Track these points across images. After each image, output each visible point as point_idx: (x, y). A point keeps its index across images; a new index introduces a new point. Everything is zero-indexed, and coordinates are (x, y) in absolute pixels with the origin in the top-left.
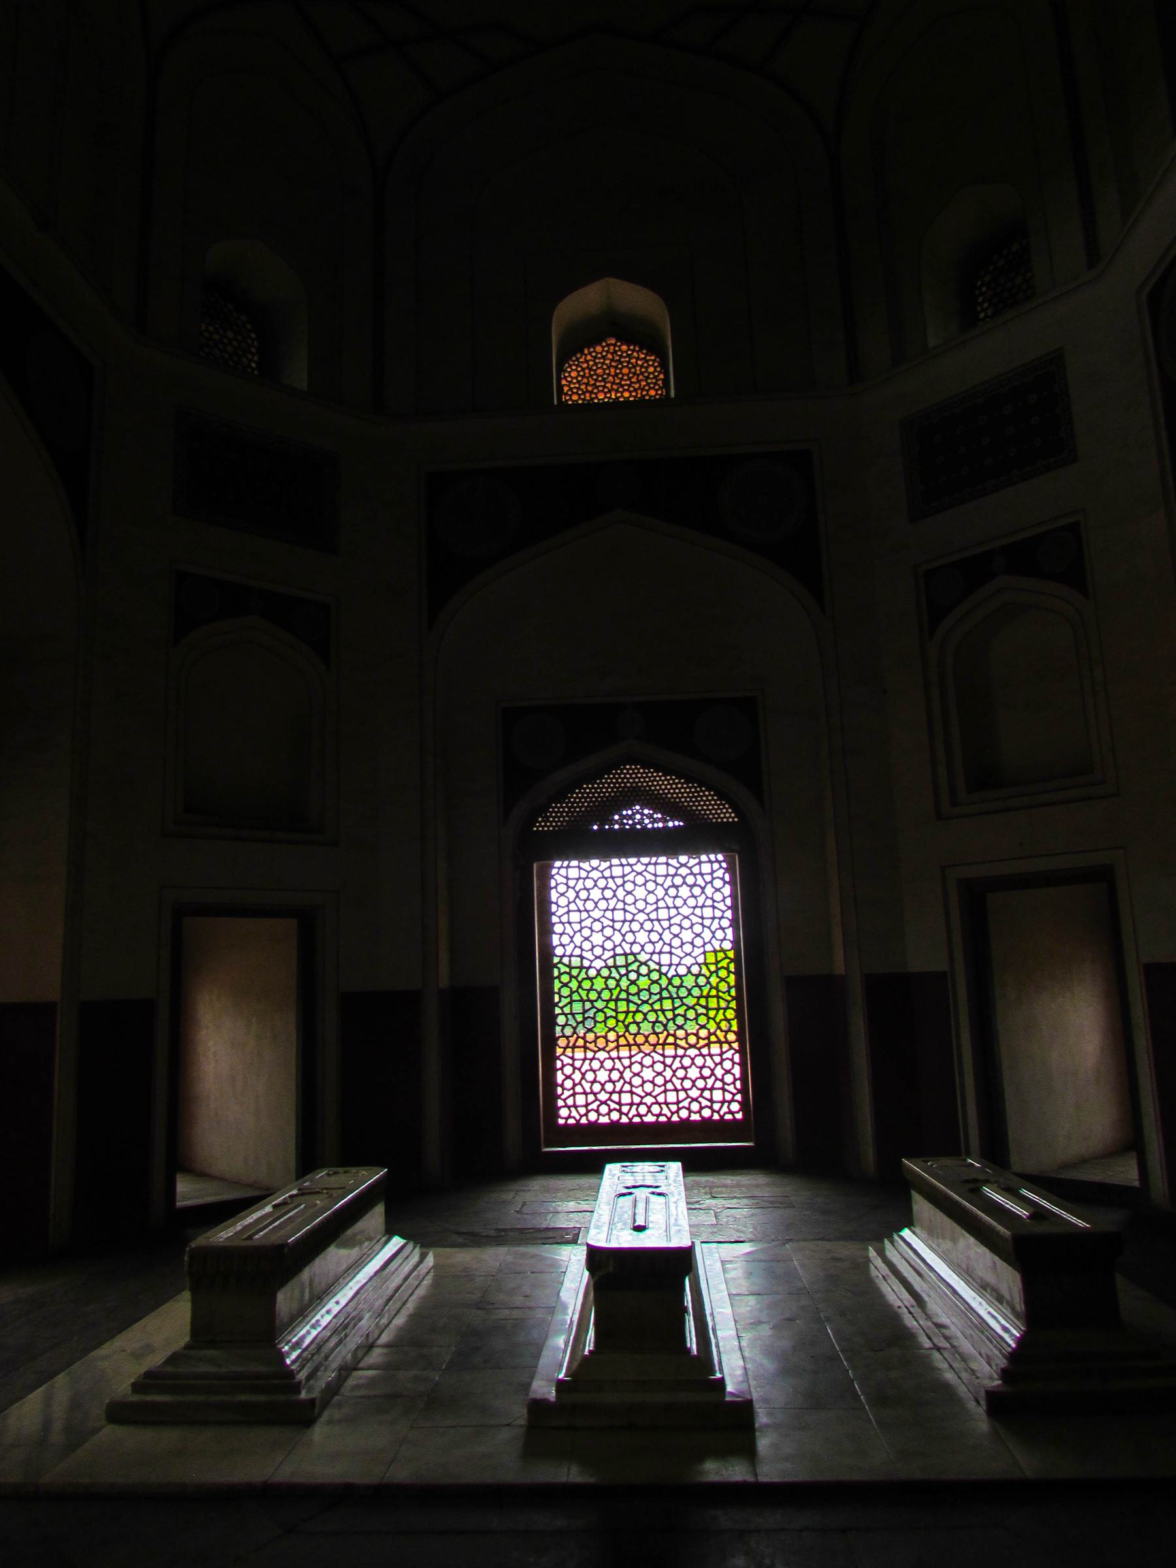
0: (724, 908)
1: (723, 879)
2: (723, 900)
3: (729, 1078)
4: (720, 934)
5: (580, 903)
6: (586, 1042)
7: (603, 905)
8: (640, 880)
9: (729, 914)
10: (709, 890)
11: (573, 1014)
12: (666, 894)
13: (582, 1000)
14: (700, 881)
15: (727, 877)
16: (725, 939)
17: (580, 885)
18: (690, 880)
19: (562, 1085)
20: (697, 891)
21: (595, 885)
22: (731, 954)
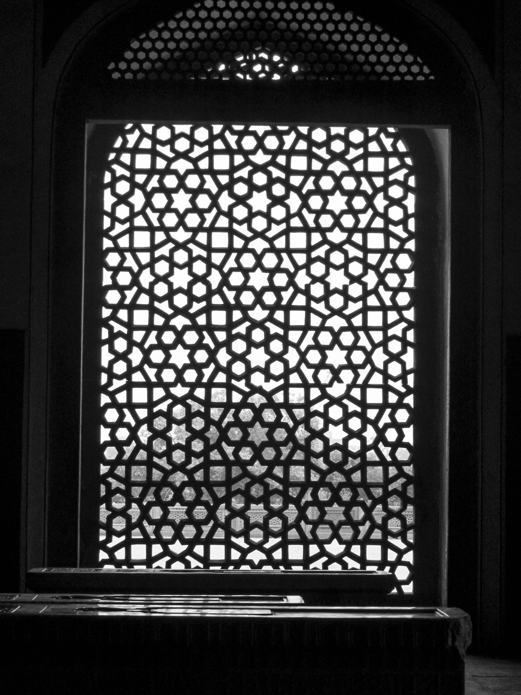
0: (404, 235)
1: (404, 184)
2: (404, 222)
3: (394, 525)
4: (393, 280)
5: (154, 217)
7: (193, 220)
8: (260, 179)
9: (411, 245)
10: (380, 202)
12: (305, 205)
14: (365, 186)
15: (412, 182)
16: (401, 288)
17: (154, 183)
18: (349, 183)
19: (108, 527)
20: (359, 203)
22: (410, 315)
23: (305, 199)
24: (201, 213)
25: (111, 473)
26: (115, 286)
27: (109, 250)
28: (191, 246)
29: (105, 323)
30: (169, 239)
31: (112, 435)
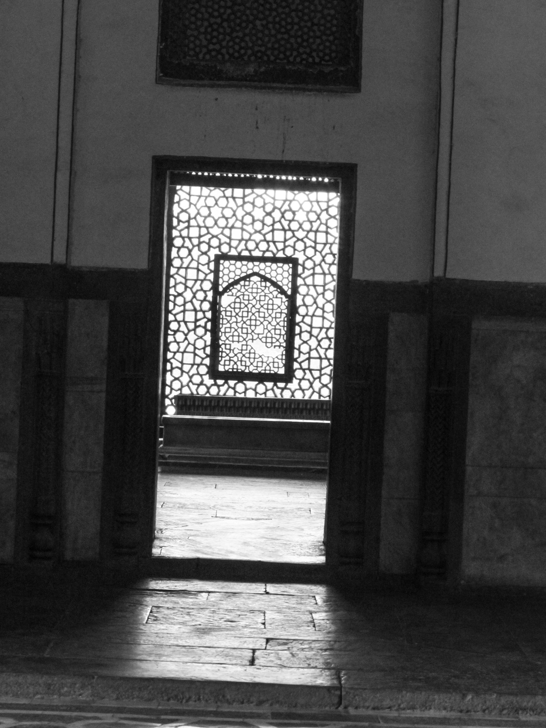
6: (195, 348)
11: (186, 323)
13: (195, 310)
14: (316, 208)
19: (170, 386)
21: (216, 204)
23: (283, 214)
24: (227, 219)
26: (179, 257)
27: (176, 237)
28: (221, 236)
30: (209, 233)
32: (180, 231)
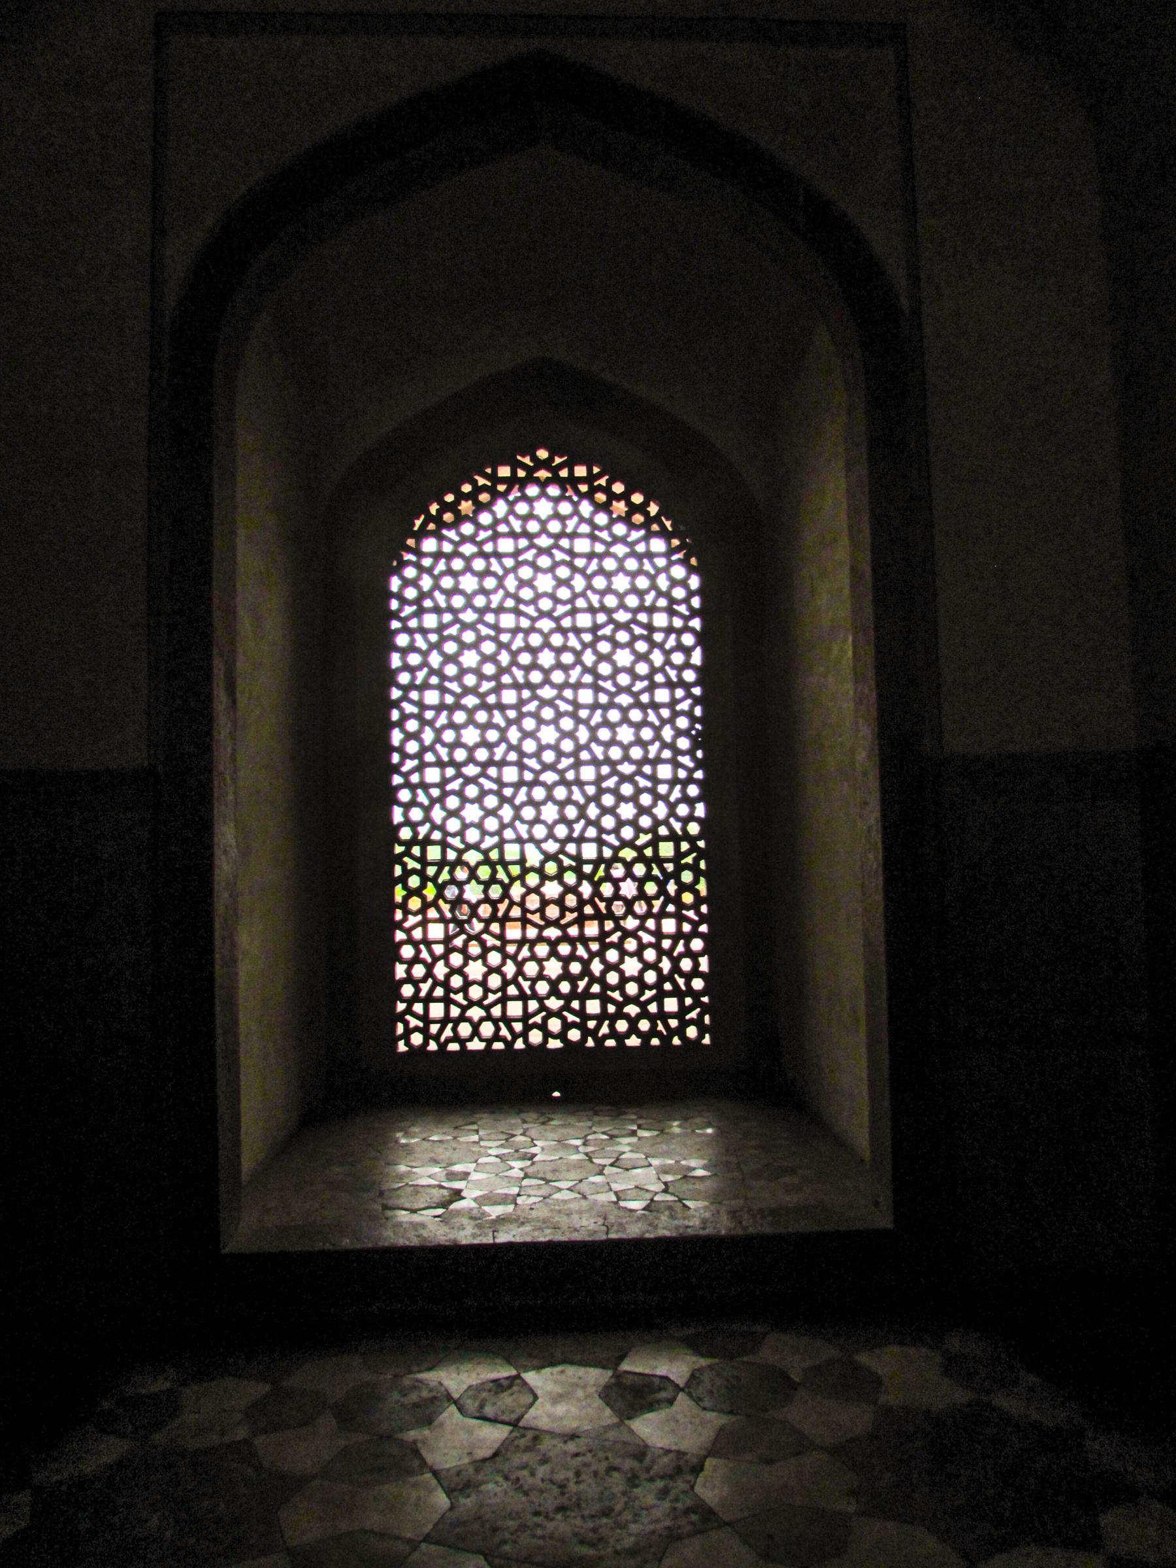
16: (691, 818)
25: (409, 1011)
26: (408, 822)
27: (400, 787)
29: (399, 859)
31: (408, 971)
32: (406, 776)
